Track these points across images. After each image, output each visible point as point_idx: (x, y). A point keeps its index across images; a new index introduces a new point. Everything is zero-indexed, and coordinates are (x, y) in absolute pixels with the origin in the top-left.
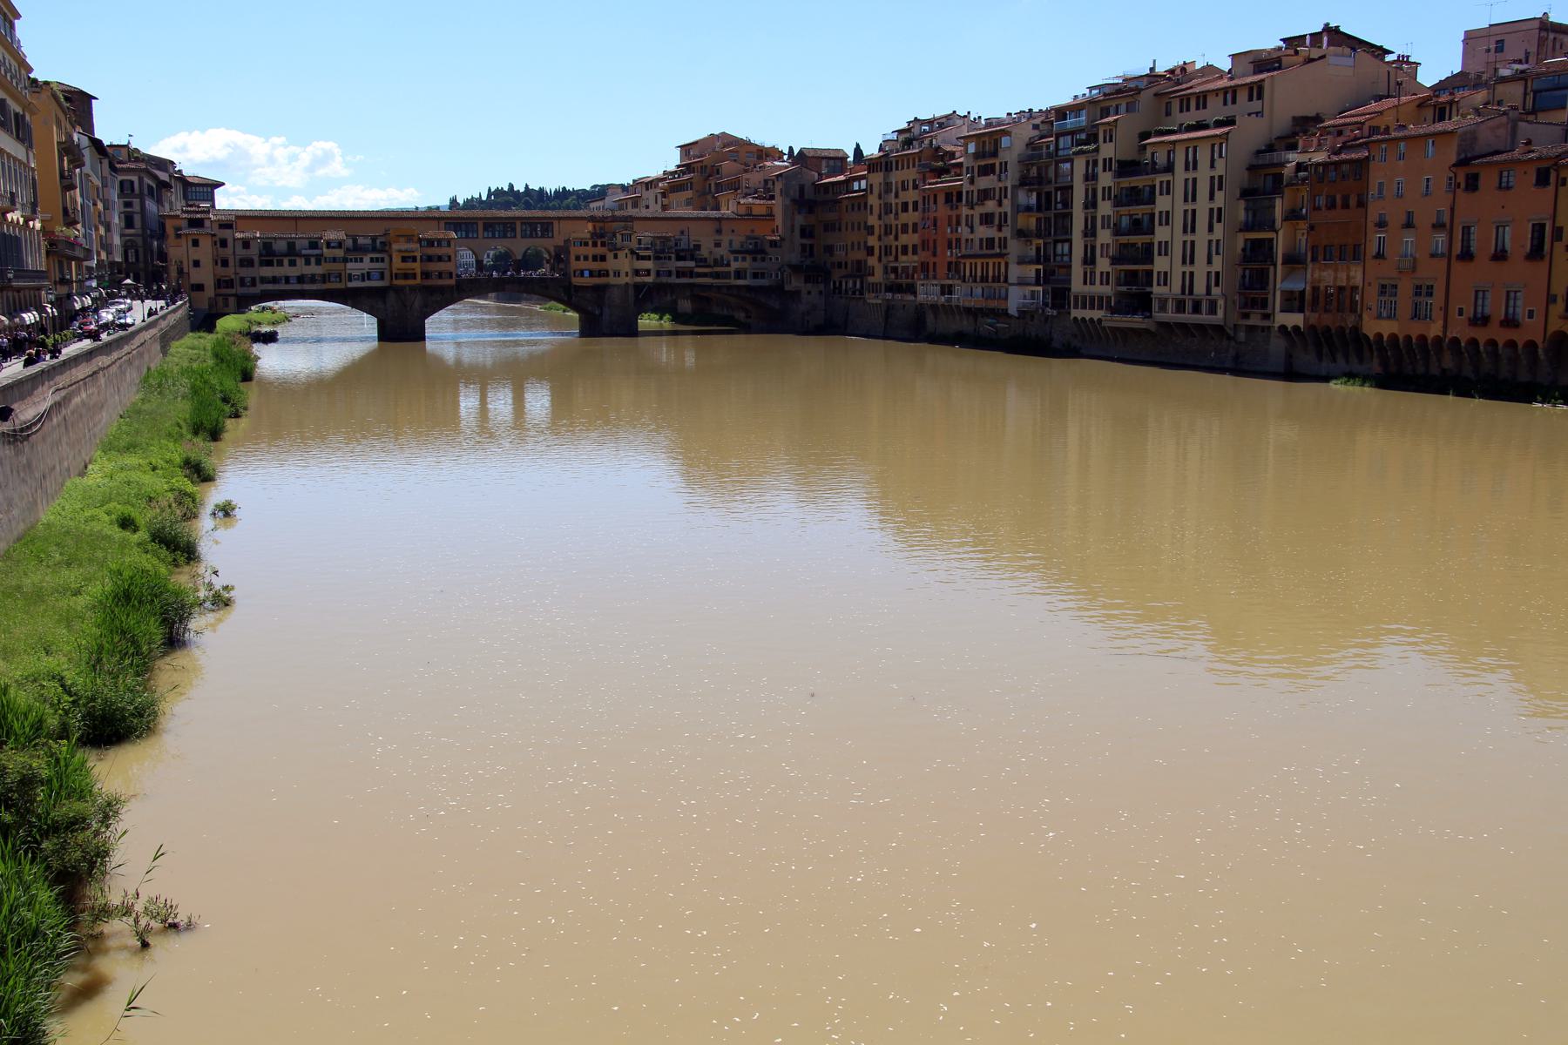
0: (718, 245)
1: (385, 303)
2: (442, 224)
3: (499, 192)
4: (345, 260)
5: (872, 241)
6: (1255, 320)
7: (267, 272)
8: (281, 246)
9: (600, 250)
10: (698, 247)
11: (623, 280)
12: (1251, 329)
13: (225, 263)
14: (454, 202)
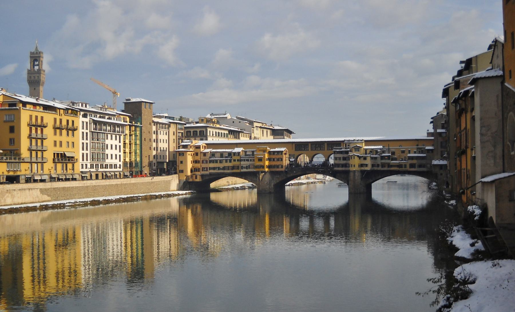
1: (256, 178)
2: (294, 145)
4: (241, 161)
7: (212, 165)
9: (345, 155)
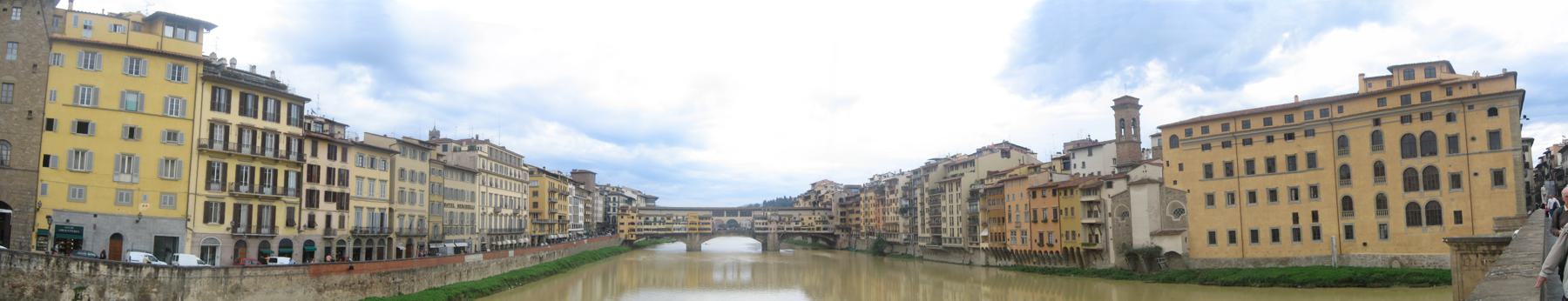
0: (810, 218)
3: (780, 199)
5: (862, 217)
6: (974, 246)
7: (646, 227)
8: (651, 219)
10: (802, 219)
11: (773, 231)
12: (974, 249)
13: (633, 224)
14: (765, 202)
